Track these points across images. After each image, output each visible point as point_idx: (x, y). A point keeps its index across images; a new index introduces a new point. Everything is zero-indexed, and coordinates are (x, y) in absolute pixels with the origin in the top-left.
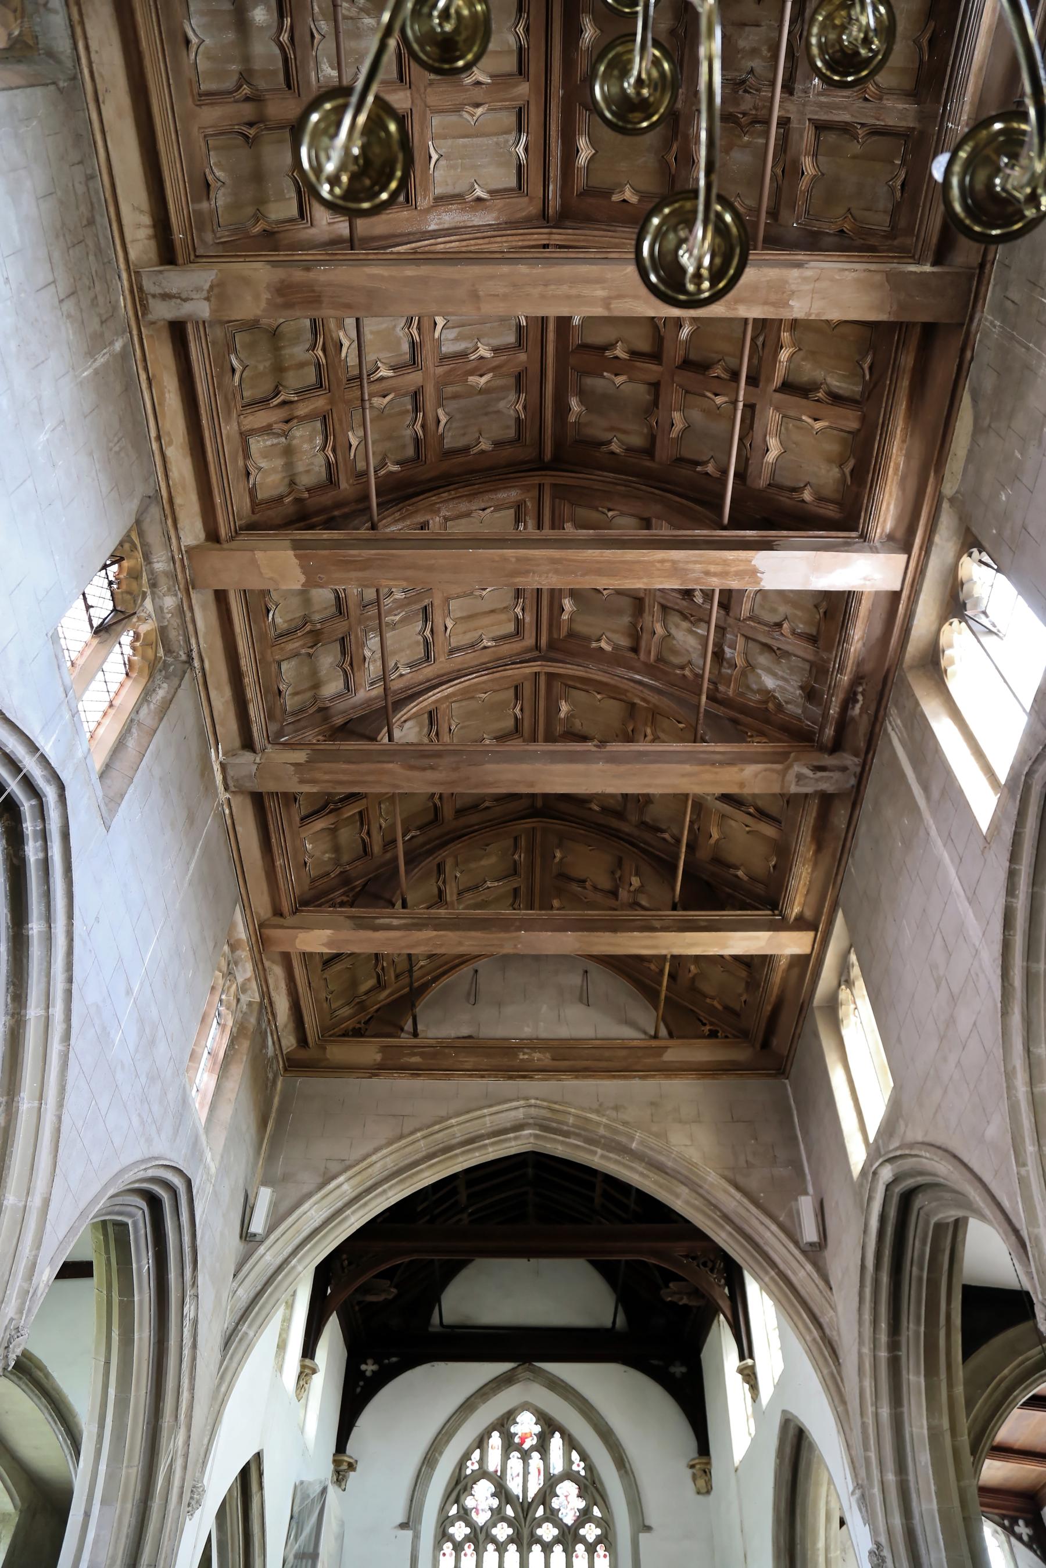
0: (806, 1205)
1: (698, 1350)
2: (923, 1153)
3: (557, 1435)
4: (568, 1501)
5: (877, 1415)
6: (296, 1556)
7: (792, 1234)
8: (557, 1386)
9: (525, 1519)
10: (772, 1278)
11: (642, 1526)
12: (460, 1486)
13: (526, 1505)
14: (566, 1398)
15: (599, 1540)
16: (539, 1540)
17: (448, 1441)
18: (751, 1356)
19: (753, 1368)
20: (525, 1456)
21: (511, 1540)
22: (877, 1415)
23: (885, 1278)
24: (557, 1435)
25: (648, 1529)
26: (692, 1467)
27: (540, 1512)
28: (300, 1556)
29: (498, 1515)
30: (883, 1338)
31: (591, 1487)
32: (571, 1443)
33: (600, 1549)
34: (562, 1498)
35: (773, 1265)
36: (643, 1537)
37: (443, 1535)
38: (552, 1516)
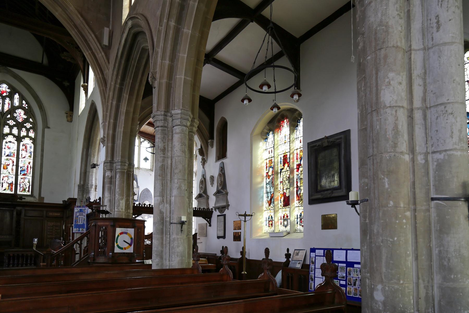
0: (106, 31)
1: (74, 79)
2: (139, 17)
3: (17, 94)
5: (112, 103)
7: (99, 39)
9: (2, 117)
10: (89, 53)
11: (46, 126)
13: (3, 114)
14: (21, 83)
18: (87, 82)
19: (87, 86)
22: (112, 103)
23: (123, 62)
25: (49, 128)
26: (67, 113)
30: (119, 81)
33: (31, 131)
35: (91, 49)
36: (46, 130)
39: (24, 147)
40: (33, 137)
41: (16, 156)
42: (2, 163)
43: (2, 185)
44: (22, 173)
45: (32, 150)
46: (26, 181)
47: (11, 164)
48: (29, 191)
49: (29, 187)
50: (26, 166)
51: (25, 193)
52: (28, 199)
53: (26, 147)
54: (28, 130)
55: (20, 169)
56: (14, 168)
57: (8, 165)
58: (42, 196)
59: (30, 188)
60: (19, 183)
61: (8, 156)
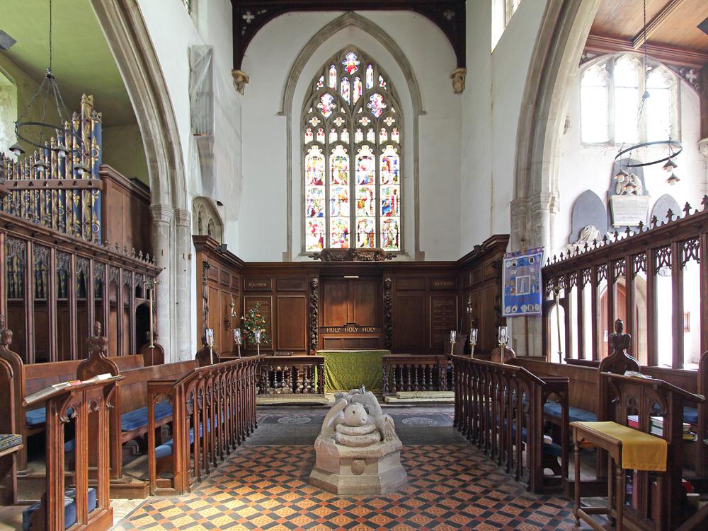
4: (377, 103)
6: (197, 94)
8: (369, 27)
12: (313, 96)
15: (394, 125)
16: (360, 126)
17: (303, 65)
20: (351, 81)
21: (344, 126)
24: (370, 66)
27: (361, 110)
28: (200, 94)
29: (336, 113)
31: (390, 96)
32: (379, 71)
33: (395, 130)
34: (373, 103)
37: (305, 124)
38: (367, 113)
39: (386, 162)
40: (398, 142)
41: (374, 183)
42: (357, 197)
43: (359, 237)
44: (386, 212)
45: (398, 167)
46: (393, 225)
47: (369, 198)
48: (397, 245)
49: (397, 236)
50: (390, 198)
51: (392, 249)
52: (400, 258)
53: (388, 164)
54: (389, 130)
55: (381, 206)
56: (374, 203)
57: (365, 200)
58: (421, 250)
59: (399, 238)
60: (381, 232)
61: (363, 183)
